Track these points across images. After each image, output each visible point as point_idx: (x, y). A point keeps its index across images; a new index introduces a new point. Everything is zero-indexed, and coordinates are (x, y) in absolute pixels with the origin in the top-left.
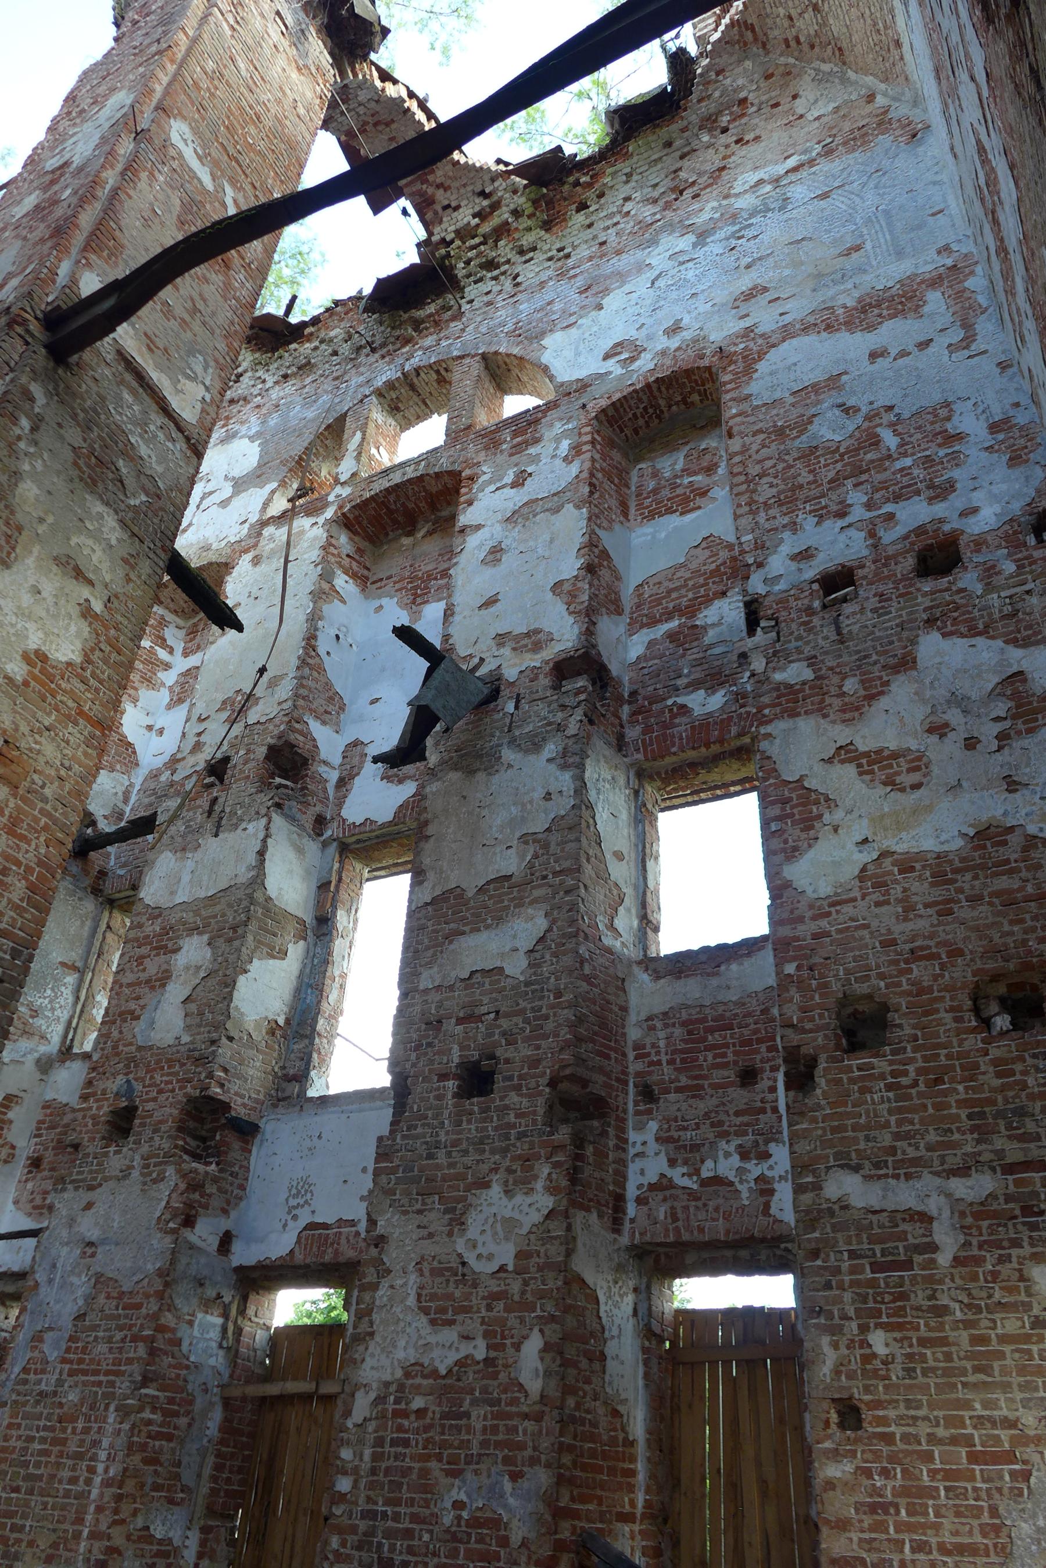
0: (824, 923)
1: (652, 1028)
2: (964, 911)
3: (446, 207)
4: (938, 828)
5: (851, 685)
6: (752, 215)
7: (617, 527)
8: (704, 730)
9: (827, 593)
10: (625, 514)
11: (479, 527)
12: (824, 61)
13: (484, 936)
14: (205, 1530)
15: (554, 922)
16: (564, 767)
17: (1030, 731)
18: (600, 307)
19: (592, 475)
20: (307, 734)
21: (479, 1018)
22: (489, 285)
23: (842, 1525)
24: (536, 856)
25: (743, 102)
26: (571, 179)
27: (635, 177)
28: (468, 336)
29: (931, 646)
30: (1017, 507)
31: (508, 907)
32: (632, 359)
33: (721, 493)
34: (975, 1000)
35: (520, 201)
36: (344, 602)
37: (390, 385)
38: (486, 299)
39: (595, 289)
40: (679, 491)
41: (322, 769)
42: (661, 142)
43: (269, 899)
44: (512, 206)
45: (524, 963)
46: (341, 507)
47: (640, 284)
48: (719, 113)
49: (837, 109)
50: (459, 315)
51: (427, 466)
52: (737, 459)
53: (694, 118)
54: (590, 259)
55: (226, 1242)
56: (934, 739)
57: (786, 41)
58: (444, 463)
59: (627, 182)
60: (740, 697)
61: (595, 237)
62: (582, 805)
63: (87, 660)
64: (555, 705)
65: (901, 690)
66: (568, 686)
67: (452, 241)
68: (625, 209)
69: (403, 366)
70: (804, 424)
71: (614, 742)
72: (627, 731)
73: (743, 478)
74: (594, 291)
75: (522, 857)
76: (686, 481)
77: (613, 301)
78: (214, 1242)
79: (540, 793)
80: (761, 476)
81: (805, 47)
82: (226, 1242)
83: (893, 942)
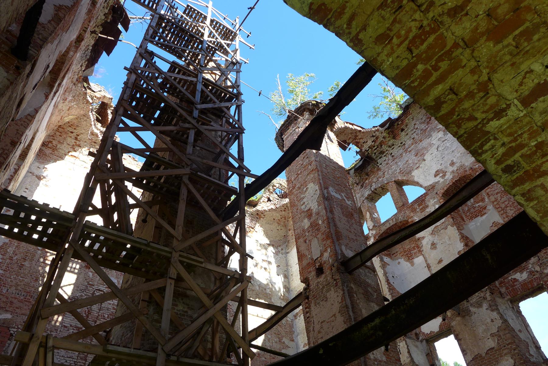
7: (464, 226)
8: (524, 284)
10: (463, 220)
11: (423, 238)
15: (515, 360)
16: (492, 310)
22: (384, 158)
24: (498, 340)
26: (396, 124)
27: (415, 118)
28: (387, 176)
31: (498, 358)
32: (444, 176)
33: (490, 207)
37: (369, 195)
38: (386, 162)
40: (476, 209)
46: (375, 237)
47: (433, 150)
50: (379, 169)
52: (495, 203)
54: (412, 144)
58: (401, 218)
60: (531, 273)
61: (410, 137)
62: (505, 321)
68: (416, 127)
71: (499, 295)
72: (501, 290)
73: (500, 209)
74: (420, 155)
75: (494, 341)
76: (477, 205)
77: (428, 157)
79: (489, 320)
80: (506, 207)
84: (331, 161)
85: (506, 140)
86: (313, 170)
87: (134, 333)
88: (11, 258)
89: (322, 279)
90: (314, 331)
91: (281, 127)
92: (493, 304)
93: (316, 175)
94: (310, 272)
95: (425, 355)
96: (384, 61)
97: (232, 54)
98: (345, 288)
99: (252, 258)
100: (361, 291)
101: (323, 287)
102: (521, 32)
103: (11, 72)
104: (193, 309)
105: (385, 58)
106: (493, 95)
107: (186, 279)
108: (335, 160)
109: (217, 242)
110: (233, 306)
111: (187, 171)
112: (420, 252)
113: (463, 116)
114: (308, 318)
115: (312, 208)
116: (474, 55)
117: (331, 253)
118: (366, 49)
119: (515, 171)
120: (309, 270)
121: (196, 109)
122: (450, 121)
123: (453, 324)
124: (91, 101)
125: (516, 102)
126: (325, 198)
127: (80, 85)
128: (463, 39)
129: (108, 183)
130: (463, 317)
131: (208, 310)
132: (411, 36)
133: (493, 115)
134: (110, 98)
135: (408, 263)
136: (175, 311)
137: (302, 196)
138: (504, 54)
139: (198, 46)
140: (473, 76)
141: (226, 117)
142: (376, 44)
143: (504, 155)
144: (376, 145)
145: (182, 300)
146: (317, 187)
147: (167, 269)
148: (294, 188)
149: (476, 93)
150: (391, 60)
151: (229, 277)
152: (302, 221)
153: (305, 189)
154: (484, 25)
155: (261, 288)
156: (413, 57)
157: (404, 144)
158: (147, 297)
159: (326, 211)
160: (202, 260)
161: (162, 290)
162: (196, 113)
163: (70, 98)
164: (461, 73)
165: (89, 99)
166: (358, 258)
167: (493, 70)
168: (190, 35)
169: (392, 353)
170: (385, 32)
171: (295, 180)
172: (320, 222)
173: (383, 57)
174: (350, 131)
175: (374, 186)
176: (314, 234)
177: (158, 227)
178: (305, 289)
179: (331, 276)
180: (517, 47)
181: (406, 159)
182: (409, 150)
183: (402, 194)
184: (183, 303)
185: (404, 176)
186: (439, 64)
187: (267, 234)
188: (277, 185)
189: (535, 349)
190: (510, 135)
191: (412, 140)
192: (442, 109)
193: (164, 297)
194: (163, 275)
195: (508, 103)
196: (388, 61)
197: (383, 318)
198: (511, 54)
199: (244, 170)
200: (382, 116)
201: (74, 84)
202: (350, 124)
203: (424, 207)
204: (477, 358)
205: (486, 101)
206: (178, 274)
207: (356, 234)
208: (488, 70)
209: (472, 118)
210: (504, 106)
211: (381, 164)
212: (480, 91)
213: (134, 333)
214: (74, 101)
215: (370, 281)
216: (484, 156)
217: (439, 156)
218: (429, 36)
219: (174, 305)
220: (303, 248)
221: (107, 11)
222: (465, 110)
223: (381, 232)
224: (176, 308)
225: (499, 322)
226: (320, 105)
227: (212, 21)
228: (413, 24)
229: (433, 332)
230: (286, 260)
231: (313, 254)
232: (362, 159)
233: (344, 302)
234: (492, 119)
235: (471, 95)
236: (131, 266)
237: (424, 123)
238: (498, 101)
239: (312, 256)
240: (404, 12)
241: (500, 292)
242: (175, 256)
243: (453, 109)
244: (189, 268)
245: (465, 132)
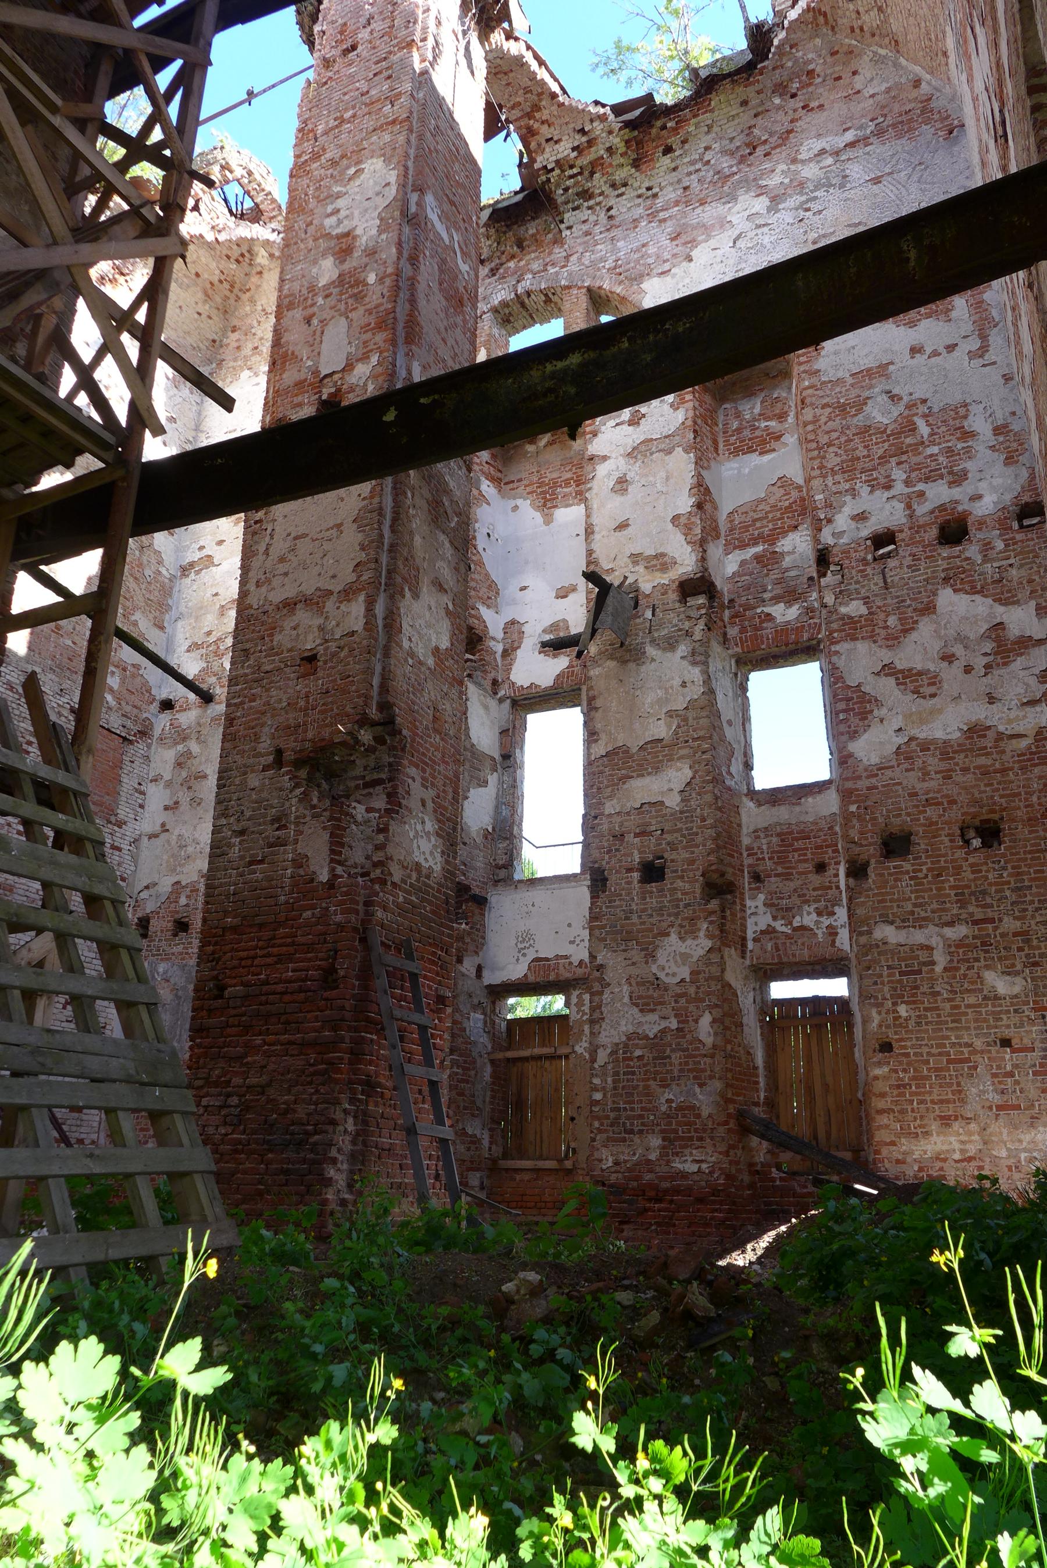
0: (874, 780)
1: (758, 837)
2: (958, 777)
3: (548, 141)
4: (947, 724)
5: (892, 621)
6: (817, 188)
7: (713, 464)
8: (783, 631)
9: (877, 549)
10: (716, 449)
11: (605, 458)
12: (881, 47)
13: (647, 780)
14: (490, 1130)
15: (696, 772)
16: (694, 663)
17: (1005, 664)
18: (690, 259)
19: (695, 423)
20: (479, 618)
21: (650, 834)
22: (585, 214)
23: (883, 1095)
24: (679, 727)
25: (810, 73)
26: (659, 123)
27: (715, 129)
28: (573, 266)
29: (946, 597)
30: (1008, 498)
33: (791, 439)
34: (961, 829)
35: (616, 141)
36: (489, 504)
37: (504, 304)
38: (585, 227)
40: (758, 433)
41: (492, 643)
42: (739, 100)
43: (473, 745)
44: (608, 145)
45: (678, 799)
47: (723, 240)
48: (791, 80)
49: (888, 90)
50: (558, 241)
52: (810, 428)
53: (769, 84)
54: (677, 203)
55: (479, 969)
56: (945, 664)
57: (852, 30)
59: (708, 132)
60: (809, 611)
61: (679, 181)
62: (711, 692)
64: (682, 616)
65: (925, 628)
66: (692, 601)
67: (553, 170)
68: (706, 158)
69: (515, 287)
70: (861, 404)
71: (721, 639)
73: (814, 445)
75: (669, 727)
76: (763, 424)
78: (473, 971)
79: (676, 682)
80: (830, 444)
81: (868, 35)
82: (479, 969)
83: (916, 794)
84: (453, 125)
86: (393, 122)
90: (267, 552)
92: (702, 649)
93: (401, 139)
95: (497, 731)
112: (581, 497)
114: (256, 522)
117: (380, 369)
120: (296, 400)
123: (594, 672)
126: (408, 218)
130: (624, 662)
137: (337, 189)
144: (579, 163)
146: (392, 177)
148: (316, 157)
152: (315, 262)
171: (326, 133)
172: (372, 278)
174: (526, 82)
176: (342, 306)
181: (644, 238)
188: (239, 172)
189: (741, 767)
191: (680, 192)
197: (592, 355)
200: (630, 83)
202: (536, 57)
204: (617, 754)
207: (456, 354)
211: (570, 228)
215: (452, 484)
217: (731, 262)
220: (296, 337)
225: (696, 691)
230: (199, 414)
231: (323, 359)
232: (522, 189)
233: (376, 500)
237: (732, 154)
241: (725, 634)
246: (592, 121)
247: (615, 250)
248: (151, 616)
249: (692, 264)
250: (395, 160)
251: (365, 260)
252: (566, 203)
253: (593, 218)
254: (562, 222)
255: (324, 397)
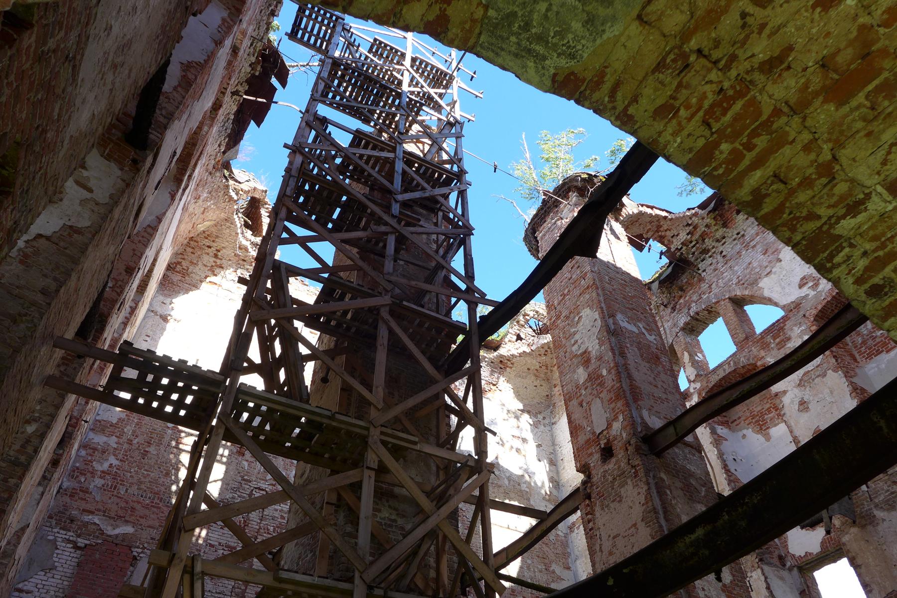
7: (857, 370)
10: (855, 360)
11: (785, 392)
22: (709, 261)
28: (715, 290)
35: (708, 221)
36: (726, 440)
37: (686, 324)
38: (712, 267)
39: (770, 251)
46: (699, 394)
50: (702, 280)
51: (735, 363)
54: (757, 234)
58: (743, 361)
63: (734, 576)
64: (889, 483)
84: (618, 270)
85: (868, 246)
86: (588, 287)
87: (317, 553)
88: (130, 442)
89: (611, 465)
90: (601, 551)
91: (532, 220)
93: (594, 294)
94: (591, 454)
96: (669, 142)
97: (448, 109)
98: (651, 480)
99: (494, 434)
100: (679, 484)
101: (614, 479)
102: (876, 87)
103: (126, 169)
104: (404, 516)
105: (669, 138)
106: (842, 180)
107: (392, 470)
108: (624, 269)
109: (438, 410)
110: (467, 511)
111: (386, 300)
112: (781, 416)
113: (798, 214)
114: (590, 530)
115: (590, 349)
116: (807, 124)
117: (625, 423)
118: (640, 127)
119: (886, 294)
121: (396, 201)
122: (779, 222)
123: (845, 539)
124: (235, 198)
125: (879, 189)
126: (611, 332)
127: (218, 174)
128: (786, 103)
129: (269, 324)
130: (863, 527)
131: (428, 517)
132: (706, 104)
133: (844, 211)
134: (263, 191)
135: (759, 436)
136: (378, 519)
138: (854, 120)
139: (393, 101)
140: (808, 154)
141: (443, 211)
142: (654, 119)
143: (867, 269)
144: (694, 239)
145: (388, 501)
146: (596, 315)
147: (362, 455)
149: (816, 179)
150: (679, 140)
151: (459, 465)
152: (574, 371)
153: (577, 318)
154: (816, 81)
155: (512, 482)
156: (712, 134)
157: (743, 235)
158: (334, 499)
159: (614, 354)
160: (417, 439)
161: (356, 487)
162: (396, 209)
163: (205, 195)
164: (788, 151)
165: (233, 194)
166: (671, 430)
167: (839, 144)
168: (382, 86)
169: (738, 589)
170: (667, 101)
171: (559, 304)
172: (604, 372)
173: (667, 136)
175: (694, 308)
176: (595, 392)
177: (346, 389)
178: (584, 483)
179: (626, 461)
180: (873, 108)
181: (748, 260)
182: (752, 244)
183: (744, 320)
184: (390, 507)
185: (746, 288)
186: (755, 141)
187: (518, 395)
190: (875, 238)
192: (764, 205)
193: (359, 498)
194: (357, 463)
195: (867, 191)
196: (675, 142)
197: (709, 527)
198: (864, 119)
199: (477, 295)
201: (210, 173)
202: (648, 207)
203: (783, 340)
205: (831, 189)
206: (380, 461)
207: (665, 389)
208: (830, 145)
209: (812, 216)
210: (861, 196)
211: (704, 271)
212: (820, 176)
213: (317, 553)
214: (211, 199)
215: (692, 468)
216: (835, 273)
218: (734, 103)
219: (376, 510)
221: (253, 59)
222: (800, 205)
223: (710, 385)
224: (379, 515)
226: (596, 180)
227: (414, 60)
228: (708, 88)
229: (810, 554)
232: (670, 263)
234: (844, 217)
235: (807, 182)
236: (307, 450)
238: (850, 189)
239: (592, 429)
240: (693, 73)
242: (375, 435)
243: (782, 204)
244: (397, 452)
245: (804, 238)
246: (691, 218)
247: (734, 273)
248: (561, 564)
249: (783, 263)
250: (595, 306)
251: (598, 363)
252: (697, 259)
253: (714, 261)
254: (698, 269)
255: (603, 446)
